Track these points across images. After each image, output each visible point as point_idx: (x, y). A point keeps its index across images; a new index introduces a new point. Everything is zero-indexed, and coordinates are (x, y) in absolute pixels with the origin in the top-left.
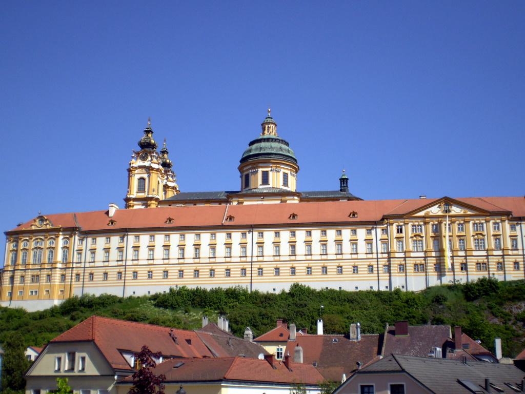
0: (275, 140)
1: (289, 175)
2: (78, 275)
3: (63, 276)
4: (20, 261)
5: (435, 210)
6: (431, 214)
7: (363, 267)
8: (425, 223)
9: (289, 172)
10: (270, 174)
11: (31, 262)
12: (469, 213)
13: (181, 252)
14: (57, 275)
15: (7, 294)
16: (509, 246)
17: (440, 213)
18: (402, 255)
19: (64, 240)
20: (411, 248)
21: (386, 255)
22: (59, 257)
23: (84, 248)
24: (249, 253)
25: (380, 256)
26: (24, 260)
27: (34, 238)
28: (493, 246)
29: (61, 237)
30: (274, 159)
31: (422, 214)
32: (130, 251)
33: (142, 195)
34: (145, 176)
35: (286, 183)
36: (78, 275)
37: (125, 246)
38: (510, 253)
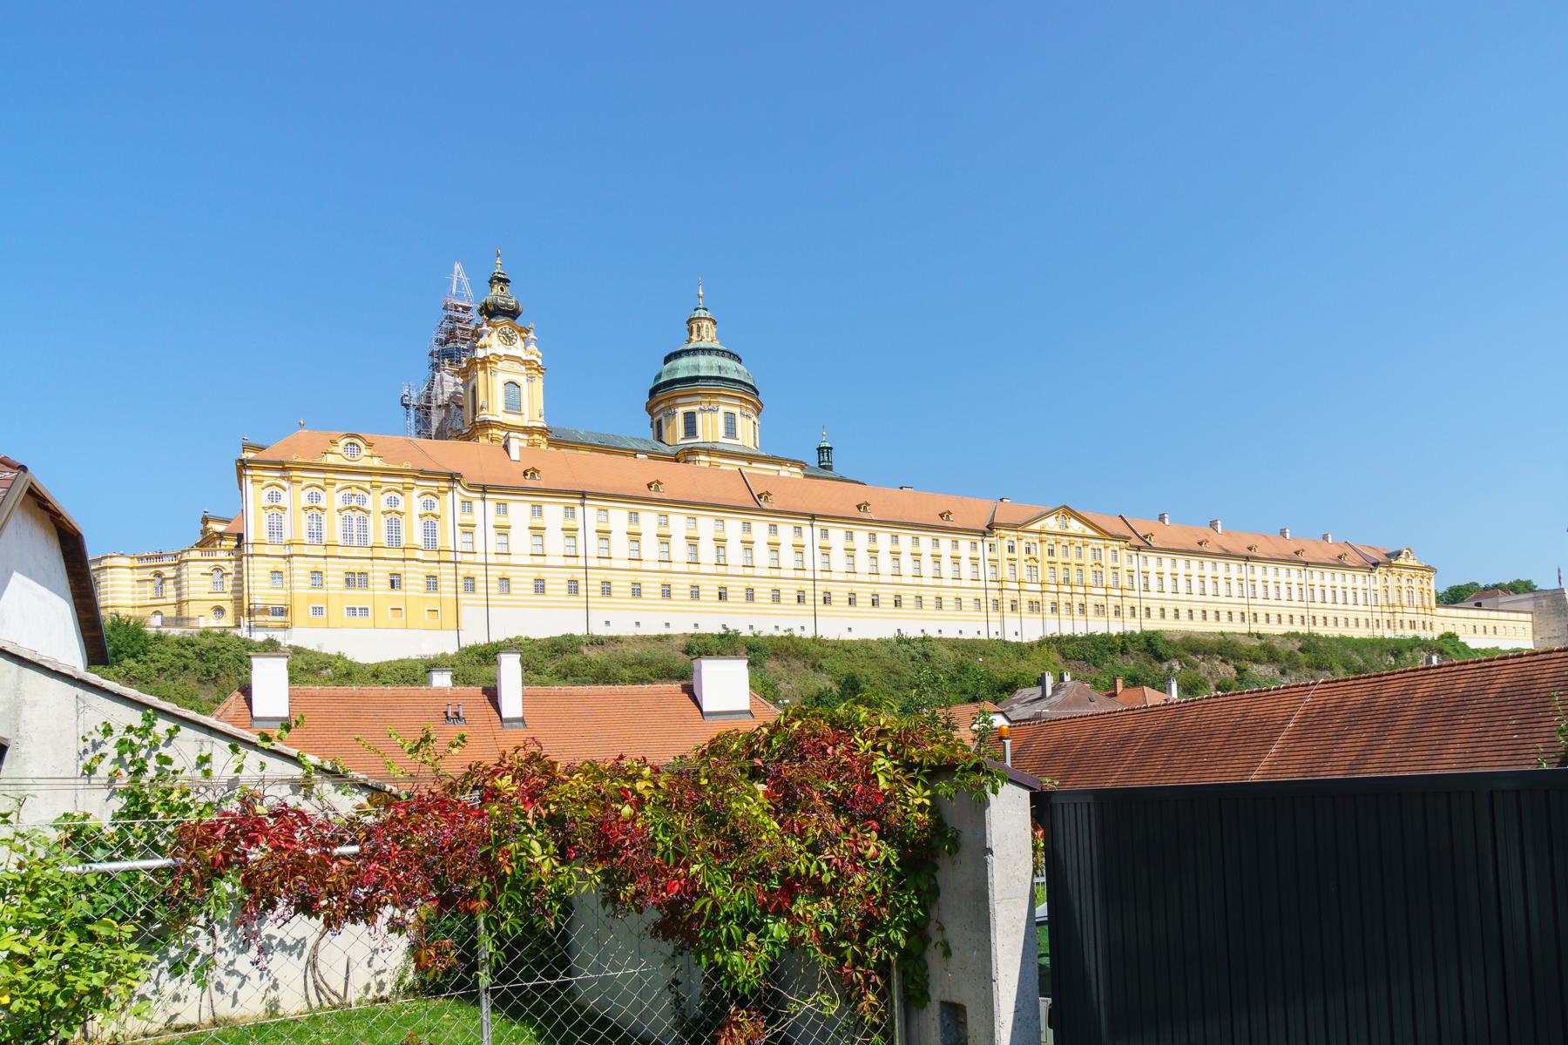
0: (704, 351)
1: (739, 419)
3: (432, 582)
5: (1051, 523)
6: (1047, 529)
9: (736, 411)
12: (1090, 532)
13: (690, 550)
14: (414, 577)
17: (1057, 529)
18: (1016, 586)
19: (424, 498)
20: (1025, 577)
21: (995, 585)
24: (808, 565)
27: (339, 485)
30: (701, 387)
31: (1036, 526)
32: (593, 538)
35: (731, 431)
36: (470, 579)
37: (580, 526)
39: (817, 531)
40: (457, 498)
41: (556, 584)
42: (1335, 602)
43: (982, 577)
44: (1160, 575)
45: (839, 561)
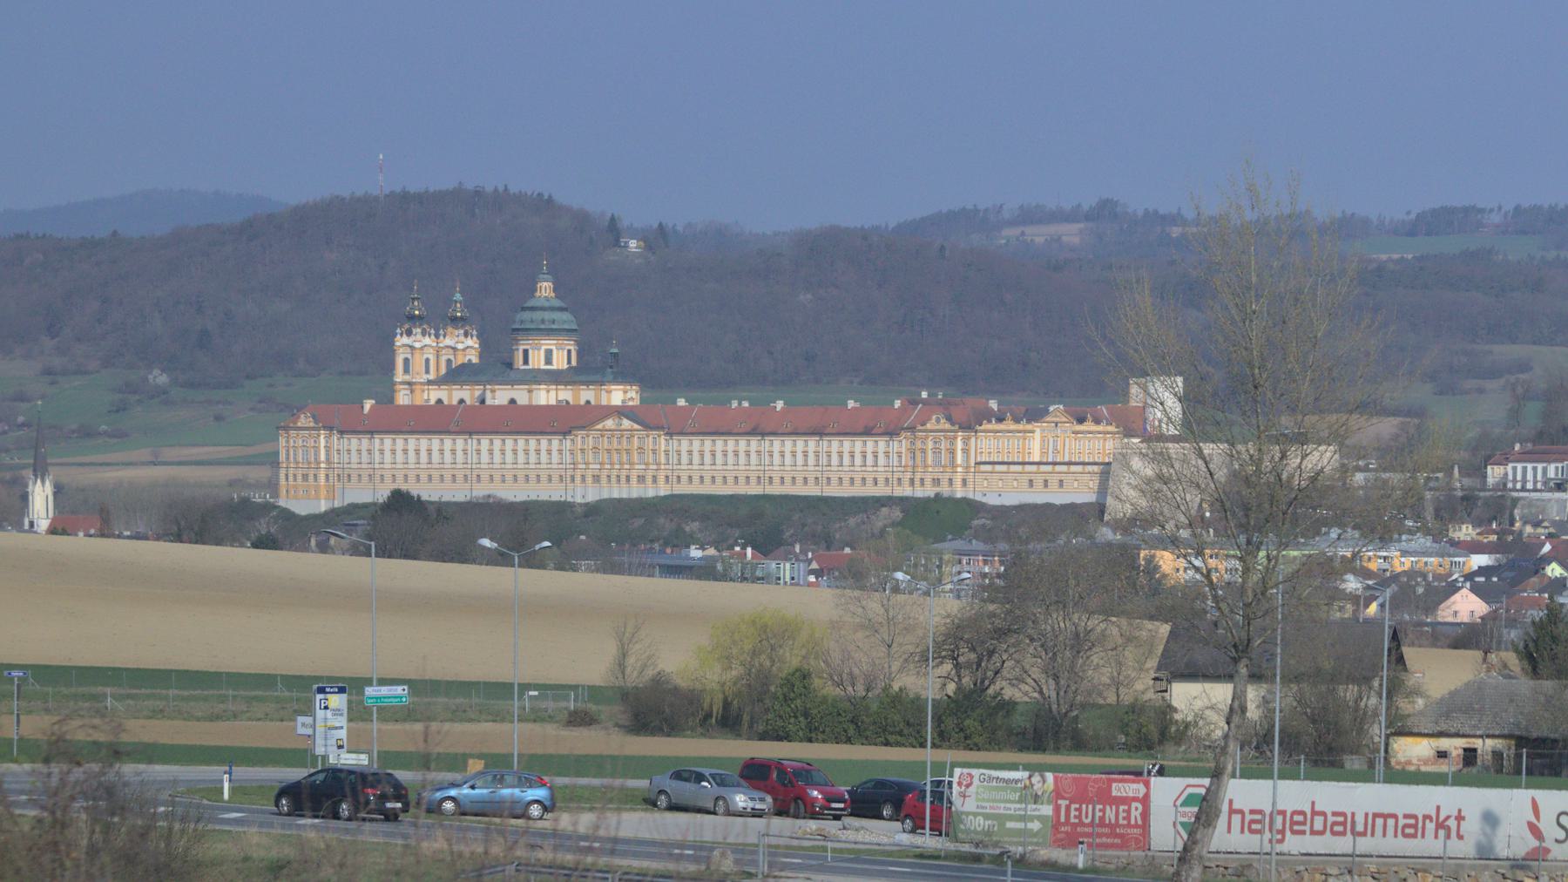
2: (339, 475)
4: (292, 459)
5: (609, 423)
8: (602, 436)
10: (530, 352)
12: (636, 426)
15: (285, 491)
16: (663, 460)
17: (613, 427)
21: (572, 466)
22: (323, 457)
24: (469, 461)
25: (568, 466)
26: (295, 458)
28: (651, 461)
29: (322, 437)
31: (600, 426)
32: (377, 453)
33: (407, 378)
34: (409, 356)
38: (663, 467)
39: (475, 441)
42: (841, 465)
43: (564, 462)
44: (690, 452)
45: (485, 457)
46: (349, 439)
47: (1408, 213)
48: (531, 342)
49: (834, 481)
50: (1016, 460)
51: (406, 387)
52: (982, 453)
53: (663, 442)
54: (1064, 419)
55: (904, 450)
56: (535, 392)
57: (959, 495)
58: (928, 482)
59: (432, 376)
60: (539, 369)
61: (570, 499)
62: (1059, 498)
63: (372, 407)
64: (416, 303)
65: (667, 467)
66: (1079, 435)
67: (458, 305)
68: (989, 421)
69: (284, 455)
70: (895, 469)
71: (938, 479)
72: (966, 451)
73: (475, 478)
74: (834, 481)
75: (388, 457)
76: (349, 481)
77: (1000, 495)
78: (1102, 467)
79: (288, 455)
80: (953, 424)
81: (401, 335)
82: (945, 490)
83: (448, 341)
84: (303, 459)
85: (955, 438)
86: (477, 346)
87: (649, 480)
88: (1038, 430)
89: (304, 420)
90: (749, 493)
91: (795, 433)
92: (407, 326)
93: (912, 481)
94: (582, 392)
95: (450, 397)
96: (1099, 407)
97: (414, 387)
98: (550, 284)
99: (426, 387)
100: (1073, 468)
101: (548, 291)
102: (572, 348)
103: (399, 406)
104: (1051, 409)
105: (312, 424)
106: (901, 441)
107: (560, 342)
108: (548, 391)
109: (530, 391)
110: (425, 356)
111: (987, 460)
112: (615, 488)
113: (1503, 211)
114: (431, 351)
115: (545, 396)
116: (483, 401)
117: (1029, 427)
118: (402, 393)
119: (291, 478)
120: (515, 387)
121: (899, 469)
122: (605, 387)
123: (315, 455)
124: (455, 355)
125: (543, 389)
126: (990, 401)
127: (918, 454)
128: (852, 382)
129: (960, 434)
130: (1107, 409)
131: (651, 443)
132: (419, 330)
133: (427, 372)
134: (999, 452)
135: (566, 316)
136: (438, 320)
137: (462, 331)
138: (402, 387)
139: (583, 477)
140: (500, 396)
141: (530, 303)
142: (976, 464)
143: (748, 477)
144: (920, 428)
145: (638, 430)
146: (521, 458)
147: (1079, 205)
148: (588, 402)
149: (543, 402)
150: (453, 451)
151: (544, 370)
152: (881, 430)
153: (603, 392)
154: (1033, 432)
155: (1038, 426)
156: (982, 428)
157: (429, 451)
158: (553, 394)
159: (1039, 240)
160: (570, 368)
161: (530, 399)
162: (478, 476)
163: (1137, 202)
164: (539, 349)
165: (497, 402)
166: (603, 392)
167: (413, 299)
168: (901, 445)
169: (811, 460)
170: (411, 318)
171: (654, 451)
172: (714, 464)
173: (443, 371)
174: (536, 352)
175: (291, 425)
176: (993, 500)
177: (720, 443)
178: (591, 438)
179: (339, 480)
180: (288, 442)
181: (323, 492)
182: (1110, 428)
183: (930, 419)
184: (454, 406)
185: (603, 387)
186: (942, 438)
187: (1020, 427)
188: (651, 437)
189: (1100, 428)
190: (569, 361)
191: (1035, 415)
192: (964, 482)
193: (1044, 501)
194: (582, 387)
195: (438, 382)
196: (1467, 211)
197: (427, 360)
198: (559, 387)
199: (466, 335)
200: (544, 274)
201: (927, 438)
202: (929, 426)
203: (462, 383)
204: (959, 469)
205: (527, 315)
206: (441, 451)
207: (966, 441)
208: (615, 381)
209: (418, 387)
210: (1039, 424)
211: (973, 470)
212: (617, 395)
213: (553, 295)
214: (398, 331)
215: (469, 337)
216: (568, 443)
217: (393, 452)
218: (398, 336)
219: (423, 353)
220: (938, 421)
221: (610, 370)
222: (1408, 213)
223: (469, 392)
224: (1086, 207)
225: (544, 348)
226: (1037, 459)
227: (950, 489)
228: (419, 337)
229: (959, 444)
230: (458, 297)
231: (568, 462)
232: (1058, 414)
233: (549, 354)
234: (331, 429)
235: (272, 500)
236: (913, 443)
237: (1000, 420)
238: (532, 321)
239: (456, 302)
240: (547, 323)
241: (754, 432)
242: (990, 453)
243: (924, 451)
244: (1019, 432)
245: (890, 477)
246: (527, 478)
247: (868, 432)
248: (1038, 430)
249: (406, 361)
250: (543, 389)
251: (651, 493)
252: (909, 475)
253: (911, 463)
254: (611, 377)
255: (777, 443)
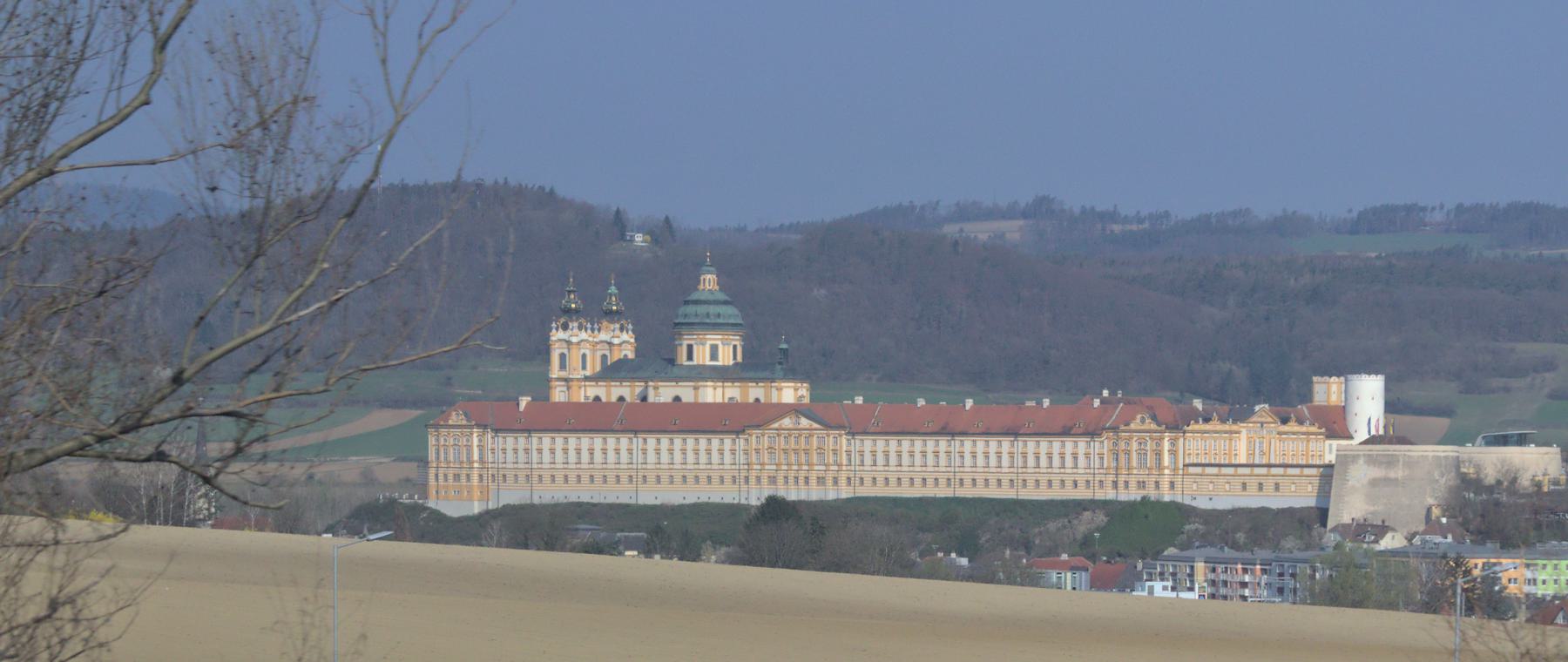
2: (493, 475)
4: (442, 458)
5: (787, 422)
6: (784, 426)
7: (728, 478)
8: (779, 435)
10: (695, 347)
11: (452, 460)
12: (816, 425)
15: (434, 493)
16: (845, 461)
17: (791, 426)
21: (746, 467)
22: (476, 457)
23: (496, 448)
24: (635, 461)
25: (742, 467)
26: (446, 458)
29: (475, 435)
31: (776, 425)
32: (535, 453)
33: (563, 374)
34: (565, 351)
38: (844, 468)
39: (640, 440)
40: (489, 436)
41: (522, 479)
42: (1038, 466)
43: (737, 462)
44: (874, 453)
45: (652, 457)
46: (504, 438)
47: (1350, 211)
48: (695, 337)
49: (1031, 484)
50: (1213, 462)
51: (563, 383)
52: (1190, 454)
53: (844, 442)
54: (1270, 419)
55: (1105, 451)
56: (700, 390)
57: (1167, 498)
58: (1133, 485)
59: (588, 373)
60: (704, 366)
61: (743, 501)
62: (1276, 502)
63: (528, 404)
64: (572, 296)
65: (849, 468)
66: (1284, 436)
67: (614, 299)
68: (1197, 422)
69: (434, 455)
70: (1096, 471)
71: (1144, 482)
72: (1173, 453)
73: (640, 479)
74: (1031, 484)
75: (547, 457)
76: (505, 481)
77: (1211, 499)
78: (1321, 469)
79: (438, 453)
80: (1159, 424)
81: (557, 329)
82: (1152, 493)
83: (603, 336)
84: (455, 457)
85: (1162, 439)
86: (632, 340)
87: (830, 482)
88: (1244, 431)
89: (455, 418)
90: (937, 496)
91: (987, 433)
92: (562, 320)
93: (1115, 484)
94: (750, 389)
95: (609, 394)
96: (1299, 407)
97: (571, 383)
98: (715, 276)
99: (583, 383)
100: (1291, 471)
101: (712, 284)
102: (737, 343)
103: (555, 403)
104: (1257, 408)
105: (464, 422)
106: (1102, 442)
107: (726, 337)
108: (715, 389)
109: (696, 388)
110: (582, 351)
111: (1195, 462)
112: (831, 491)
113: (1445, 210)
114: (629, 347)
115: (712, 394)
116: (644, 399)
117: (1235, 428)
118: (558, 389)
119: (441, 478)
120: (680, 384)
121: (1101, 471)
122: (776, 384)
123: (468, 454)
124: (611, 350)
125: (710, 386)
126: (1195, 401)
127: (1122, 457)
128: (870, 379)
129: (1166, 434)
130: (1308, 408)
131: (742, 444)
132: (576, 324)
133: (584, 368)
134: (1284, 454)
135: (730, 310)
136: (594, 314)
137: (618, 326)
138: (557, 383)
139: (758, 479)
140: (663, 393)
141: (694, 296)
142: (1184, 466)
143: (924, 479)
144: (1122, 428)
145: (815, 429)
146: (691, 458)
147: (1016, 202)
148: (757, 400)
149: (710, 399)
150: (617, 451)
151: (710, 366)
152: (1080, 431)
153: (773, 390)
154: (1239, 432)
155: (1244, 427)
156: (1190, 428)
157: (591, 452)
158: (720, 391)
159: (983, 237)
160: (736, 364)
161: (696, 396)
162: (961, 480)
163: (1074, 198)
164: (704, 344)
165: (657, 400)
166: (773, 390)
167: (570, 292)
168: (1102, 445)
169: (1005, 461)
170: (567, 311)
171: (835, 452)
172: (875, 465)
173: (598, 368)
174: (701, 347)
175: (442, 423)
176: (1203, 504)
177: (906, 443)
178: (766, 438)
179: (493, 481)
180: (438, 440)
181: (477, 493)
182: (1313, 429)
183: (1134, 419)
184: (751, 404)
185: (773, 384)
186: (1148, 439)
187: (1227, 427)
188: (832, 436)
189: (1304, 429)
190: (735, 358)
191: (1241, 415)
192: (1172, 485)
193: (1260, 506)
194: (750, 384)
195: (594, 378)
196: (1410, 209)
197: (584, 356)
198: (726, 384)
199: (622, 329)
200: (707, 266)
201: (1130, 438)
202: (1133, 426)
203: (621, 380)
204: (1166, 471)
205: (690, 309)
206: (604, 451)
207: (1173, 442)
208: (786, 378)
209: (575, 383)
210: (1245, 425)
211: (1181, 472)
212: (789, 393)
213: (717, 287)
214: (554, 325)
215: (625, 332)
216: (741, 443)
217: (552, 451)
218: (554, 331)
219: (580, 349)
220: (1143, 421)
221: (780, 367)
222: (1350, 211)
223: (628, 389)
224: (1023, 205)
225: (709, 343)
226: (1243, 461)
227: (1156, 492)
228: (618, 332)
229: (1166, 445)
230: (613, 289)
231: (741, 462)
232: (1264, 414)
233: (714, 349)
234: (483, 426)
235: (421, 501)
236: (1115, 444)
237: (1207, 420)
238: (696, 315)
239: (611, 295)
240: (712, 317)
241: (943, 432)
242: (1198, 454)
243: (1128, 453)
244: (1226, 432)
245: (1091, 479)
246: (658, 478)
247: (1066, 432)
248: (1244, 431)
249: (563, 356)
250: (710, 386)
251: (831, 496)
252: (1111, 478)
253: (1113, 464)
254: (781, 373)
255: (968, 443)
